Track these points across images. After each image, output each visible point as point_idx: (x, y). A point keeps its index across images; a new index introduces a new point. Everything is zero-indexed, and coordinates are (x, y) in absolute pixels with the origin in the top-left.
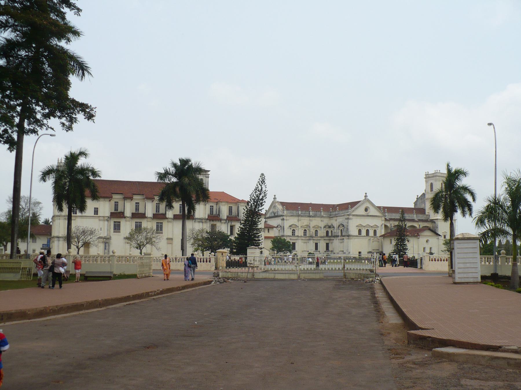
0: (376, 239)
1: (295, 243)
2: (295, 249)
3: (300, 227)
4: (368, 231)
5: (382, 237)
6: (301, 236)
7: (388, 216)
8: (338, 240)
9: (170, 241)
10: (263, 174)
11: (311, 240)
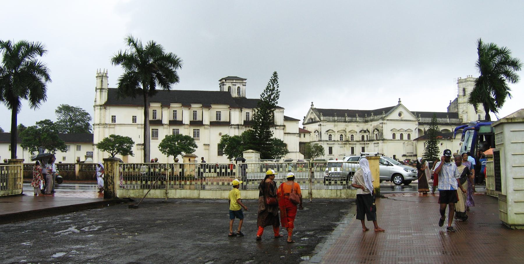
1: (332, 147)
2: (332, 154)
3: (336, 132)
4: (402, 135)
5: (416, 141)
6: (338, 141)
7: (421, 120)
8: (373, 144)
9: (207, 147)
10: (275, 73)
11: (347, 144)
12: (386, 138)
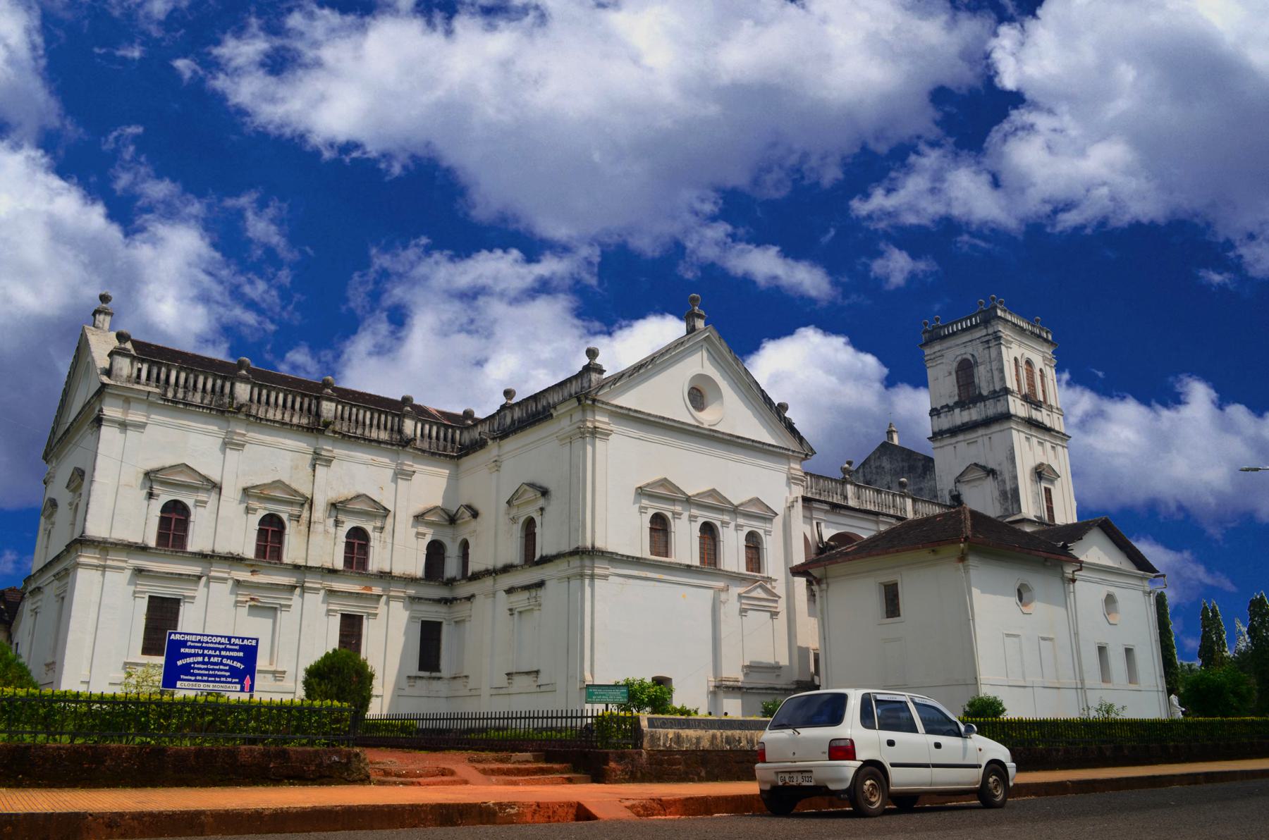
0: (759, 593)
3: (231, 492)
6: (235, 560)
12: (599, 544)
